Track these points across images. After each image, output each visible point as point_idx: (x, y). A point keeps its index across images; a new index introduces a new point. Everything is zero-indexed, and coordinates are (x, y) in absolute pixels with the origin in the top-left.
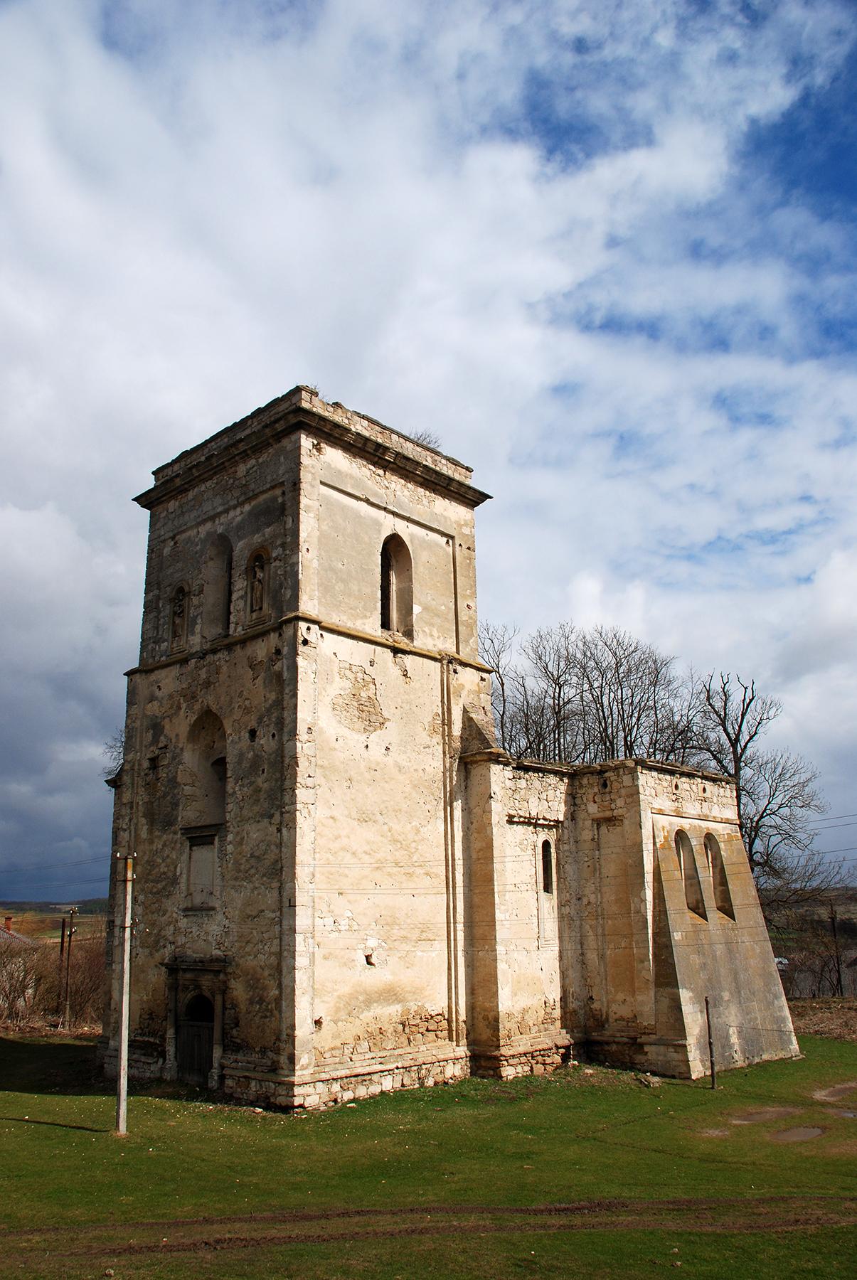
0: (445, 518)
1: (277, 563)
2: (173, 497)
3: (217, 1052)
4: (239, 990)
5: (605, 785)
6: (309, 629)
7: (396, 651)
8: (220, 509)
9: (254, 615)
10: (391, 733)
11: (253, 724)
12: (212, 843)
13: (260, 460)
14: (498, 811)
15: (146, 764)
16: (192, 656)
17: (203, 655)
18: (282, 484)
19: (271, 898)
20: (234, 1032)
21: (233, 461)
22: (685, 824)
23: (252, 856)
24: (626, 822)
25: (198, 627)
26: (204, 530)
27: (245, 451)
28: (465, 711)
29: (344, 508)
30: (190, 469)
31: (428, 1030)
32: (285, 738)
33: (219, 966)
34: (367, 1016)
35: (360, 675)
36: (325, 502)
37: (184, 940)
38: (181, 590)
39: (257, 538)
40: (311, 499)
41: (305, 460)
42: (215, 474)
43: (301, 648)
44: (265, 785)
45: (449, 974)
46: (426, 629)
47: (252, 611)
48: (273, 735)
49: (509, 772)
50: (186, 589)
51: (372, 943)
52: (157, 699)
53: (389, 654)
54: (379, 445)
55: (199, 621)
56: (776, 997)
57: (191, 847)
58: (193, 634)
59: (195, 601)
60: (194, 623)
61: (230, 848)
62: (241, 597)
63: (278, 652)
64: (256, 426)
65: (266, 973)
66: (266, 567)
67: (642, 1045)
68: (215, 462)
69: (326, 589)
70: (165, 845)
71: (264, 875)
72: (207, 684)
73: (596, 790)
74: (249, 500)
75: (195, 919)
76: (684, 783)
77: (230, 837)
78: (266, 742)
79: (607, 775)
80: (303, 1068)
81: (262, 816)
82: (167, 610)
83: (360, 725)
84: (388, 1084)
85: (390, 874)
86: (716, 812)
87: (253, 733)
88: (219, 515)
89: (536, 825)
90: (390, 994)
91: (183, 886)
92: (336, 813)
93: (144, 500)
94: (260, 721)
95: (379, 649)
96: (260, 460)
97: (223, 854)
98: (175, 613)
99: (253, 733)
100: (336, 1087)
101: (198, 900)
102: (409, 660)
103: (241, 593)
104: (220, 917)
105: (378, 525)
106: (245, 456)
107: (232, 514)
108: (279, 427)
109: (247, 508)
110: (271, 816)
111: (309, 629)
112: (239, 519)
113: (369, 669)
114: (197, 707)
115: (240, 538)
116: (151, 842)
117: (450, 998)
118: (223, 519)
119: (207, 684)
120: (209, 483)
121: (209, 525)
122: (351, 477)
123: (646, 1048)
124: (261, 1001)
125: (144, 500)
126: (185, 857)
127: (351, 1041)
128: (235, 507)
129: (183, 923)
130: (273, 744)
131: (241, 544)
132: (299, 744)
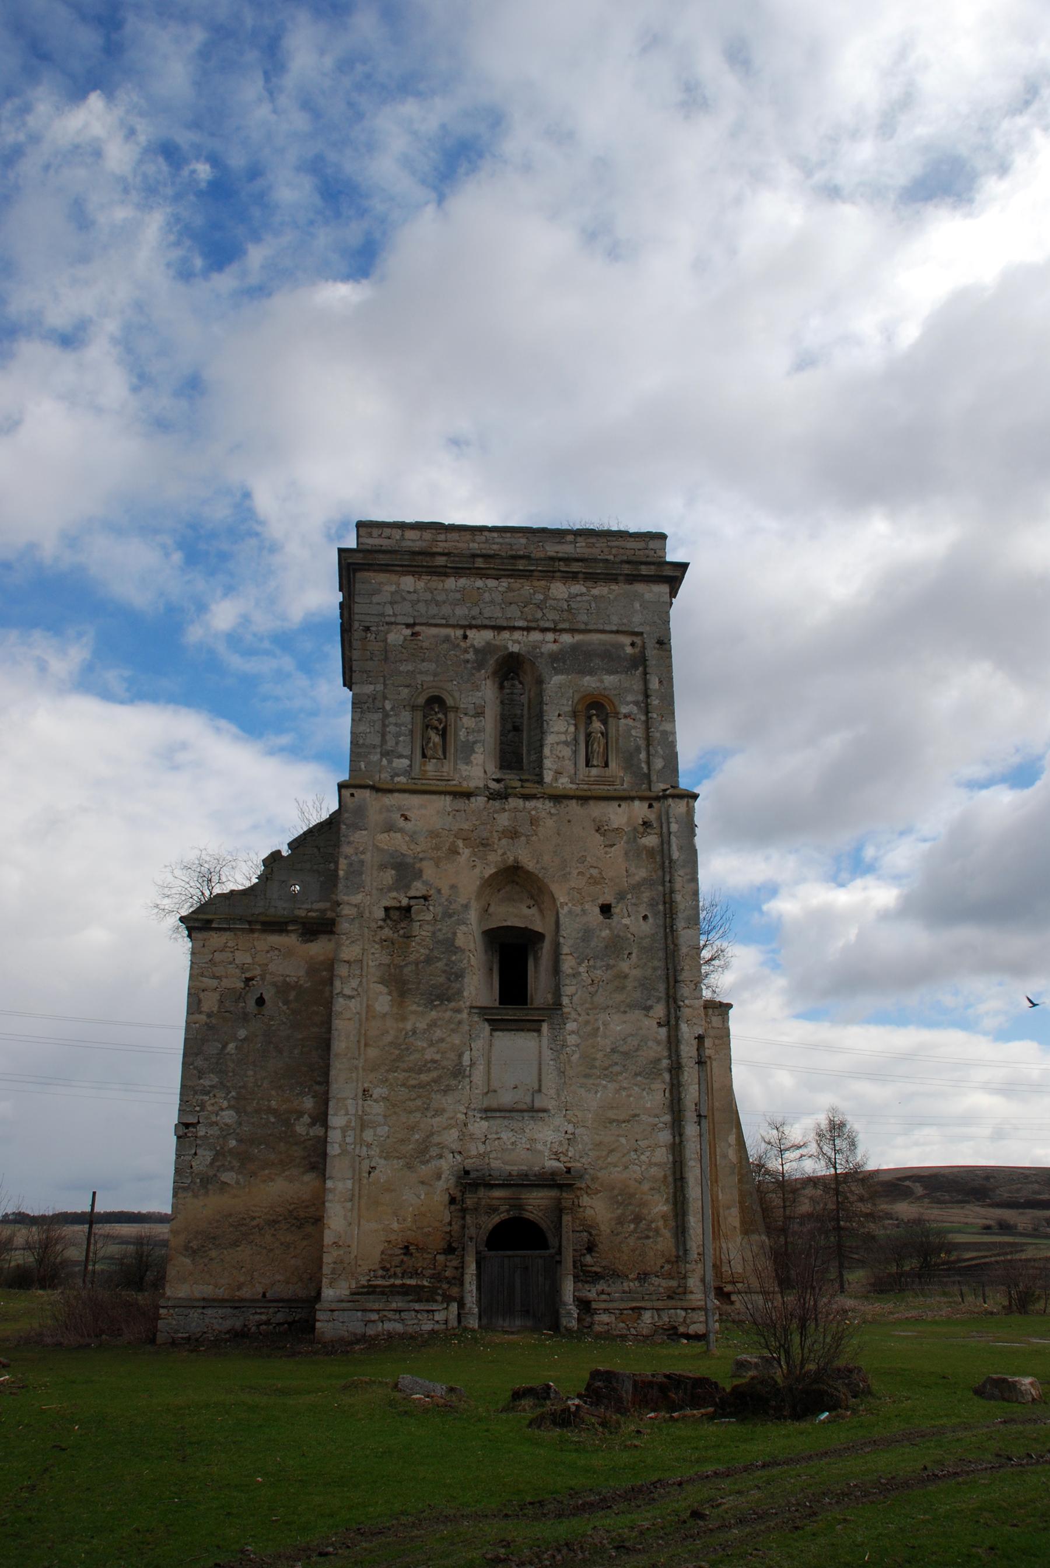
1: (629, 722)
4: (597, 1209)
9: (594, 771)
11: (608, 898)
12: (538, 1031)
13: (595, 592)
20: (588, 1259)
21: (549, 575)
25: (478, 758)
26: (479, 638)
27: (578, 573)
30: (474, 556)
32: (680, 924)
33: (562, 1182)
37: (482, 1149)
39: (589, 682)
48: (645, 917)
50: (450, 702)
52: (401, 830)
55: (479, 749)
57: (492, 1030)
58: (468, 763)
61: (572, 1040)
62: (566, 743)
64: (581, 548)
65: (646, 1187)
66: (611, 721)
68: (521, 565)
70: (433, 1024)
71: (636, 1075)
74: (573, 631)
75: (506, 1122)
77: (571, 1026)
81: (633, 1006)
87: (606, 910)
88: (514, 628)
91: (478, 1075)
94: (621, 896)
104: (558, 1121)
106: (574, 577)
107: (536, 636)
108: (644, 570)
109: (566, 638)
112: (554, 647)
114: (494, 858)
115: (557, 671)
118: (517, 635)
119: (513, 834)
120: (491, 583)
121: (488, 635)
124: (638, 1219)
128: (544, 630)
129: (479, 1127)
130: (646, 928)
131: (557, 679)
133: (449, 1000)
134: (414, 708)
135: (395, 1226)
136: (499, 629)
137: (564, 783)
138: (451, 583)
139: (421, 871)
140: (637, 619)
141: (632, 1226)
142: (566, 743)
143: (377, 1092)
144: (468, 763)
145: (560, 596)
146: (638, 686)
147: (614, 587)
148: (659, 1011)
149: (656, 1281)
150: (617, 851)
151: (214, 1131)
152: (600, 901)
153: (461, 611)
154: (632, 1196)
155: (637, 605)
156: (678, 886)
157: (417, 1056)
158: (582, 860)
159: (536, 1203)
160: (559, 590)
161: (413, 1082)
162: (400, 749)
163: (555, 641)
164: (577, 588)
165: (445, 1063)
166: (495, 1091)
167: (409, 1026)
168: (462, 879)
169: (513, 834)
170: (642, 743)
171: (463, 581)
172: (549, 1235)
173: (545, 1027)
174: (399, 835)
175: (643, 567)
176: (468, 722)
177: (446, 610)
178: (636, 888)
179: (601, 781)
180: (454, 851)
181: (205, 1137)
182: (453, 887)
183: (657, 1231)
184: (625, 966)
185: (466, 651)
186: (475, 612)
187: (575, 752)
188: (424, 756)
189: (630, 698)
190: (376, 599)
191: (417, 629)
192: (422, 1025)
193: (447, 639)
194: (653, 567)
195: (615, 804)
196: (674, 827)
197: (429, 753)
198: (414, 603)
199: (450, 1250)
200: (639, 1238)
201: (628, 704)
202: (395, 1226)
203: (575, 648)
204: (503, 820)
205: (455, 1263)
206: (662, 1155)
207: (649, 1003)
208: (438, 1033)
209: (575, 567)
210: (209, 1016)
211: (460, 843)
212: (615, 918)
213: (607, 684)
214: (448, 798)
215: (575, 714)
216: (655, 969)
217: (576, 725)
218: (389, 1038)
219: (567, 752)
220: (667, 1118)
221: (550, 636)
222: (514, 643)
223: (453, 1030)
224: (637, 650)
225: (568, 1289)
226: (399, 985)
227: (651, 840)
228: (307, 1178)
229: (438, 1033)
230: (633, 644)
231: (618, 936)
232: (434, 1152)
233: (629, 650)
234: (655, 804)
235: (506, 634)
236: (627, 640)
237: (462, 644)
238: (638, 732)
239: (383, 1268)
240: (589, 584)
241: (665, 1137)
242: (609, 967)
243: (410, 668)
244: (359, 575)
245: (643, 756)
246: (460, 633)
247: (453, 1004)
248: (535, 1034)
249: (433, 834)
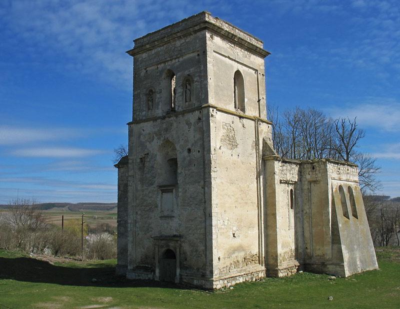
0: (255, 63)
2: (145, 52)
3: (178, 271)
4: (186, 247)
5: (314, 168)
6: (213, 110)
7: (241, 117)
8: (169, 59)
9: (187, 103)
10: (239, 150)
11: (190, 146)
14: (277, 178)
15: (139, 160)
16: (159, 118)
17: (164, 118)
18: (198, 51)
19: (200, 213)
20: (185, 263)
21: (174, 39)
22: (342, 183)
23: (191, 197)
24: (321, 182)
25: (160, 107)
26: (161, 66)
28: (264, 140)
29: (221, 61)
31: (252, 260)
32: (205, 153)
33: (177, 237)
34: (234, 256)
35: (229, 127)
36: (215, 59)
38: (151, 91)
39: (187, 72)
40: (211, 57)
41: (208, 42)
42: (166, 44)
43: (211, 118)
45: (259, 240)
46: (249, 108)
47: (186, 102)
48: (199, 151)
49: (280, 164)
50: (154, 91)
51: (235, 229)
53: (237, 119)
54: (233, 35)
56: (371, 247)
58: (158, 109)
59: (158, 96)
60: (158, 103)
61: (180, 194)
63: (199, 119)
67: (326, 265)
69: (217, 94)
71: (196, 205)
72: (166, 130)
73: (310, 170)
76: (341, 167)
77: (180, 190)
78: (196, 154)
79: (314, 164)
80: (216, 275)
82: (144, 98)
83: (230, 147)
84: (241, 280)
85: (240, 203)
86: (352, 178)
87: (189, 150)
89: (288, 184)
90: (240, 248)
92: (223, 181)
93: (132, 53)
95: (235, 117)
96: (187, 41)
97: (177, 197)
98: (149, 100)
99: (189, 150)
100: (226, 282)
101: (166, 213)
102: (244, 120)
103: (180, 94)
105: (232, 66)
106: (180, 38)
107: (174, 61)
108: (196, 28)
110: (199, 182)
111: (213, 110)
113: (232, 125)
114: (162, 139)
116: (143, 191)
117: (259, 248)
119: (166, 130)
120: (162, 48)
121: (163, 65)
122: (224, 48)
123: (328, 266)
124: (196, 251)
125: (132, 53)
126: (159, 197)
127: (229, 265)
128: (175, 59)
132: (211, 155)
133: (153, 185)
136: (164, 62)
138: (153, 52)
141: (195, 253)
143: (139, 212)
144: (158, 109)
145: (178, 46)
147: (192, 37)
148: (202, 183)
152: (187, 148)
158: (183, 134)
160: (178, 43)
161: (146, 209)
163: (179, 61)
164: (183, 41)
166: (163, 211)
168: (154, 147)
170: (200, 89)
171: (156, 50)
173: (174, 190)
175: (196, 27)
176: (158, 96)
178: (196, 142)
185: (158, 73)
187: (183, 98)
191: (148, 69)
192: (147, 193)
194: (198, 26)
195: (191, 114)
200: (197, 257)
207: (199, 180)
208: (150, 195)
209: (179, 34)
210: (122, 191)
211: (155, 135)
212: (191, 153)
215: (182, 85)
217: (183, 89)
221: (177, 60)
222: (168, 65)
226: (142, 181)
229: (150, 195)
230: (198, 55)
232: (150, 229)
237: (157, 71)
240: (186, 38)
241: (204, 224)
242: (189, 170)
243: (145, 82)
248: (171, 193)
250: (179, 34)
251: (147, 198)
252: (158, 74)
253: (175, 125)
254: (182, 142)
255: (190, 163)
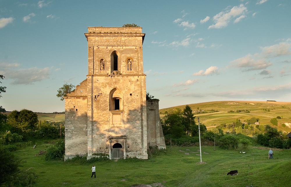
5: (152, 104)
39: (128, 55)
44: (135, 105)
62: (124, 66)
67: (157, 146)
73: (150, 104)
87: (131, 94)
91: (111, 122)
96: (129, 39)
107: (119, 47)
108: (138, 35)
109: (124, 47)
118: (116, 47)
119: (116, 83)
120: (111, 38)
121: (111, 47)
123: (158, 147)
124: (136, 143)
126: (111, 117)
134: (99, 61)
135: (99, 145)
137: (124, 73)
139: (101, 89)
140: (137, 44)
142: (124, 66)
146: (137, 56)
149: (138, 152)
150: (133, 85)
151: (71, 130)
153: (106, 43)
154: (135, 139)
155: (136, 41)
156: (142, 91)
157: (101, 119)
158: (127, 86)
159: (120, 141)
160: (123, 39)
162: (97, 68)
164: (126, 38)
165: (105, 120)
167: (100, 115)
169: (116, 83)
170: (137, 66)
171: (106, 38)
172: (122, 146)
174: (97, 83)
177: (103, 43)
178: (136, 91)
179: (130, 72)
180: (106, 86)
181: (69, 131)
182: (106, 92)
183: (139, 144)
184: (134, 104)
186: (108, 44)
188: (101, 70)
189: (135, 58)
190: (91, 42)
191: (99, 47)
192: (102, 114)
193: (104, 48)
195: (132, 77)
196: (142, 81)
197: (101, 69)
198: (98, 42)
199: (107, 148)
201: (135, 59)
202: (99, 145)
203: (126, 50)
204: (114, 80)
205: (108, 150)
206: (140, 133)
208: (104, 116)
211: (107, 84)
213: (131, 56)
214: (105, 77)
216: (139, 104)
218: (97, 116)
219: (125, 68)
220: (141, 127)
221: (122, 47)
223: (107, 115)
224: (137, 49)
225: (125, 153)
227: (138, 83)
228: (86, 137)
229: (104, 116)
231: (133, 99)
233: (135, 49)
234: (139, 76)
235: (114, 47)
236: (135, 47)
238: (137, 64)
239: (97, 151)
240: (128, 37)
241: (140, 130)
244: (88, 37)
245: (137, 68)
246: (106, 47)
247: (106, 111)
249: (103, 83)
250: (126, 35)
251: (102, 117)
252: (107, 51)
253: (121, 81)
254: (126, 90)
255: (132, 101)
